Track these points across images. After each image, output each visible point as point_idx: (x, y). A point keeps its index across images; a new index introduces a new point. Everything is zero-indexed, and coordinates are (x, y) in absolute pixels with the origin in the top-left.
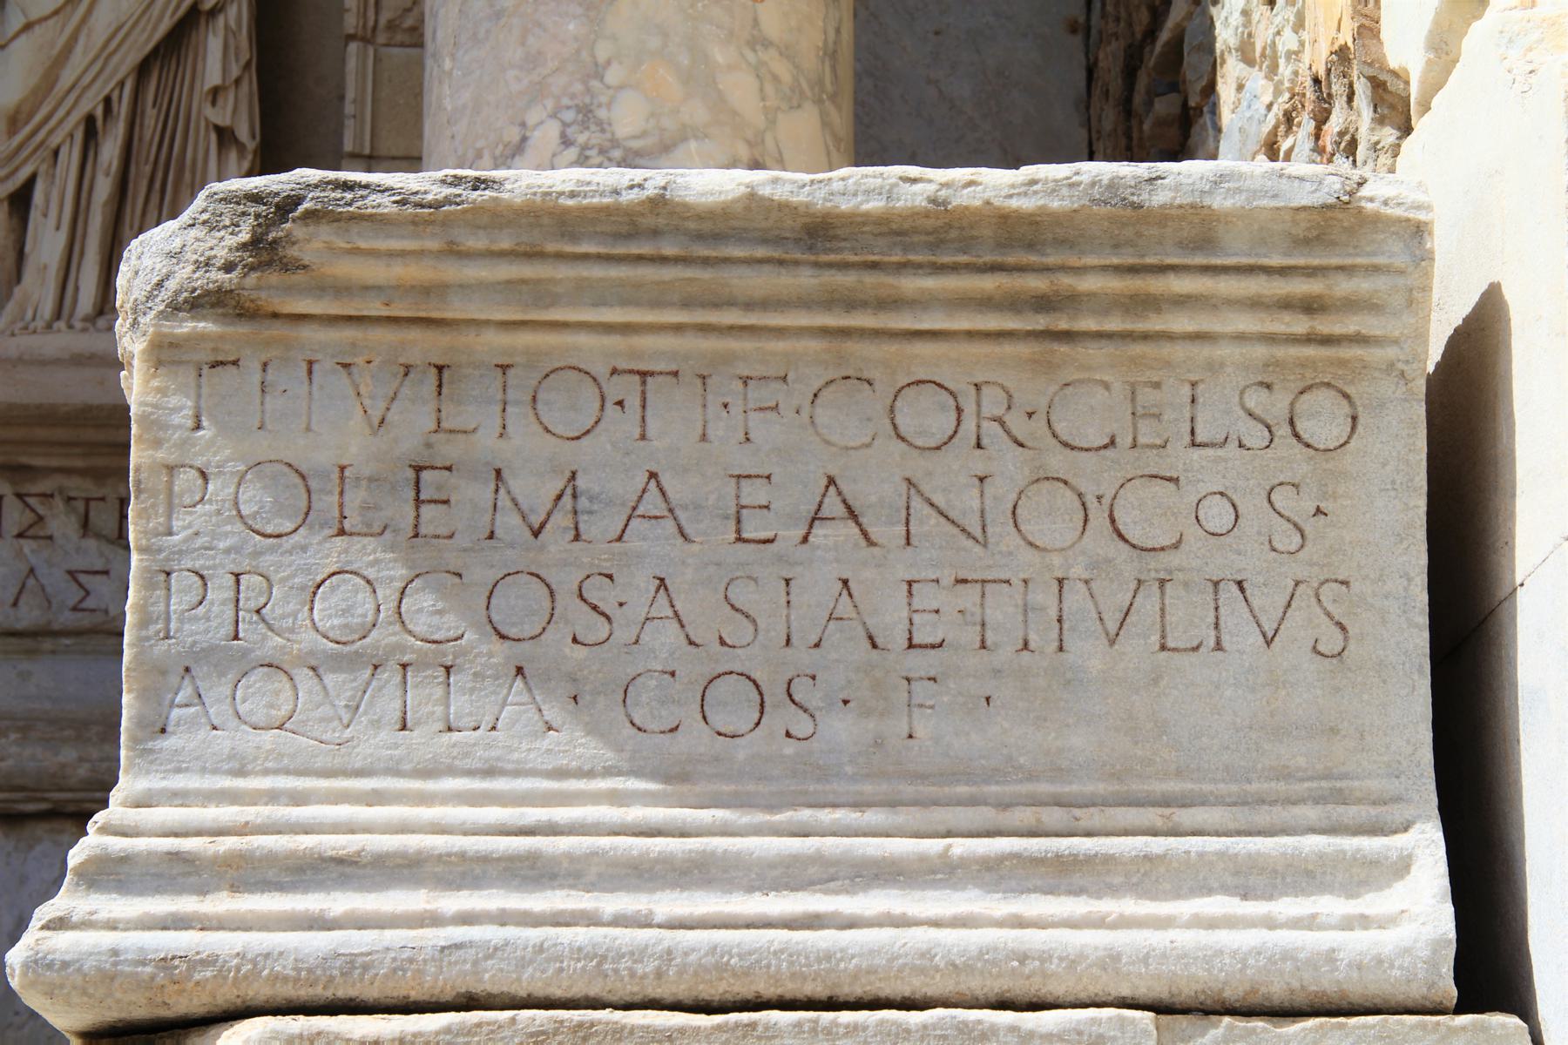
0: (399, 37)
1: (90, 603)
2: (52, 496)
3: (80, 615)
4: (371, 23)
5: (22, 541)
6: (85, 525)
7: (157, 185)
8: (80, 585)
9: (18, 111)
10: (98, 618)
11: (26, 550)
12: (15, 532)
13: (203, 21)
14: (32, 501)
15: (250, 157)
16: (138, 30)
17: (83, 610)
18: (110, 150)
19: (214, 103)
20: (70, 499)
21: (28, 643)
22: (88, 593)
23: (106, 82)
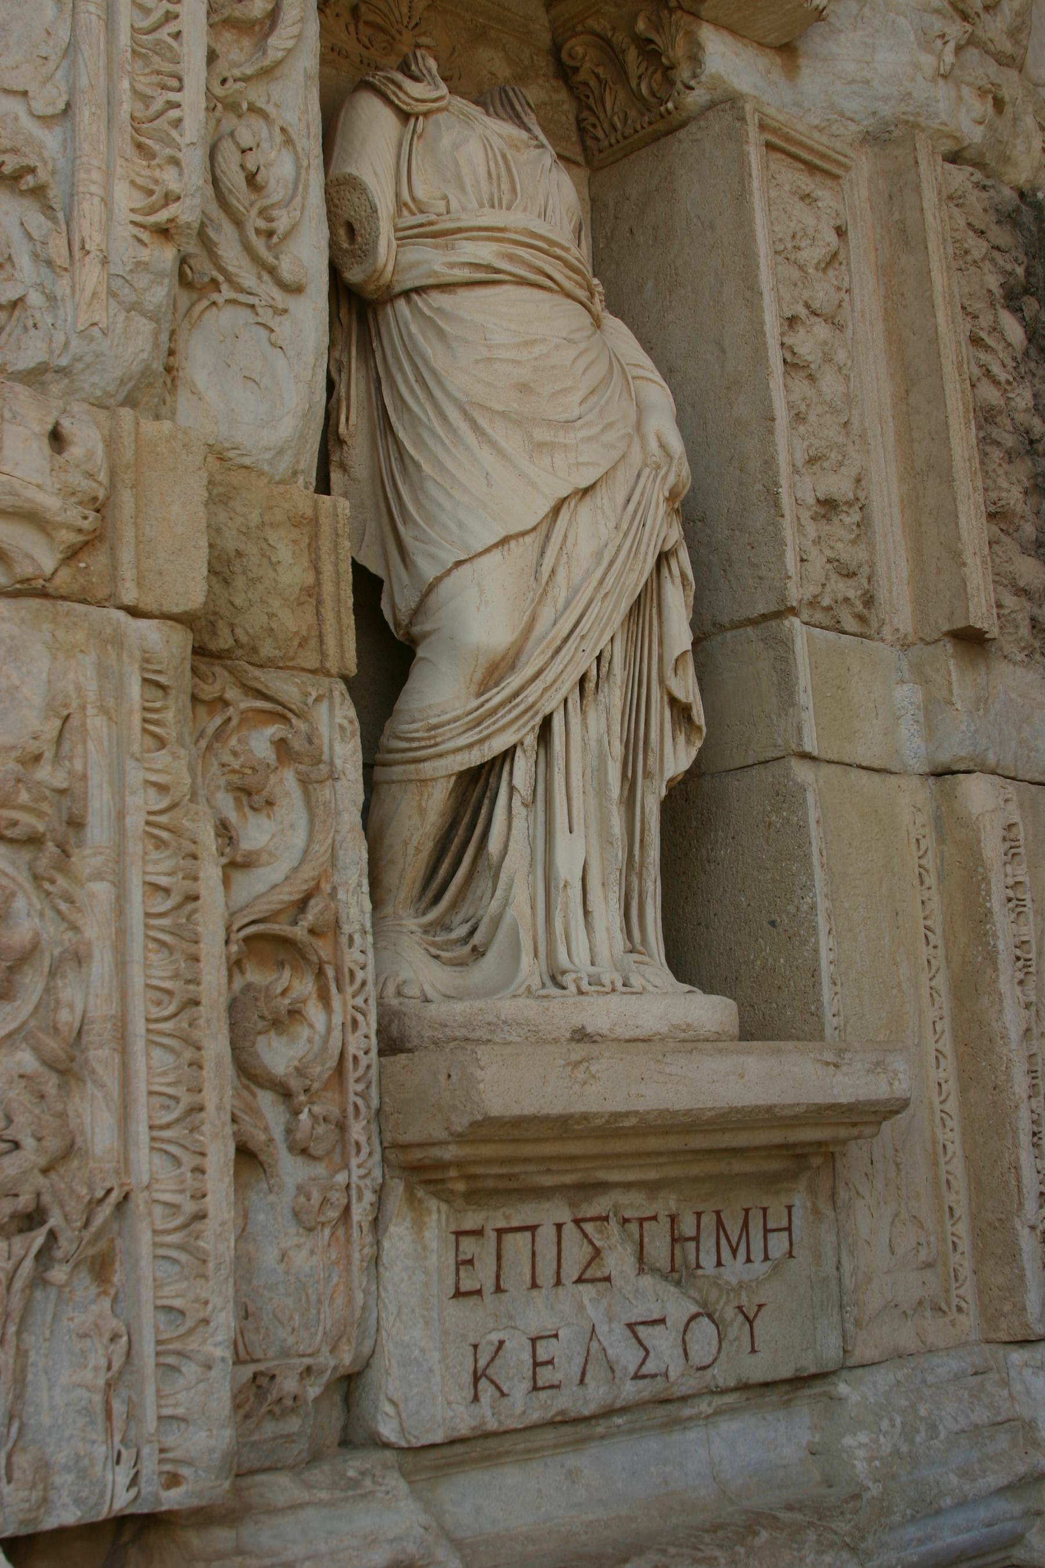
1: (650, 1367)
2: (606, 1219)
3: (641, 1383)
5: (581, 1287)
8: (640, 1342)
10: (659, 1384)
12: (575, 1277)
14: (589, 1227)
15: (699, 744)
17: (644, 1377)
20: (626, 1221)
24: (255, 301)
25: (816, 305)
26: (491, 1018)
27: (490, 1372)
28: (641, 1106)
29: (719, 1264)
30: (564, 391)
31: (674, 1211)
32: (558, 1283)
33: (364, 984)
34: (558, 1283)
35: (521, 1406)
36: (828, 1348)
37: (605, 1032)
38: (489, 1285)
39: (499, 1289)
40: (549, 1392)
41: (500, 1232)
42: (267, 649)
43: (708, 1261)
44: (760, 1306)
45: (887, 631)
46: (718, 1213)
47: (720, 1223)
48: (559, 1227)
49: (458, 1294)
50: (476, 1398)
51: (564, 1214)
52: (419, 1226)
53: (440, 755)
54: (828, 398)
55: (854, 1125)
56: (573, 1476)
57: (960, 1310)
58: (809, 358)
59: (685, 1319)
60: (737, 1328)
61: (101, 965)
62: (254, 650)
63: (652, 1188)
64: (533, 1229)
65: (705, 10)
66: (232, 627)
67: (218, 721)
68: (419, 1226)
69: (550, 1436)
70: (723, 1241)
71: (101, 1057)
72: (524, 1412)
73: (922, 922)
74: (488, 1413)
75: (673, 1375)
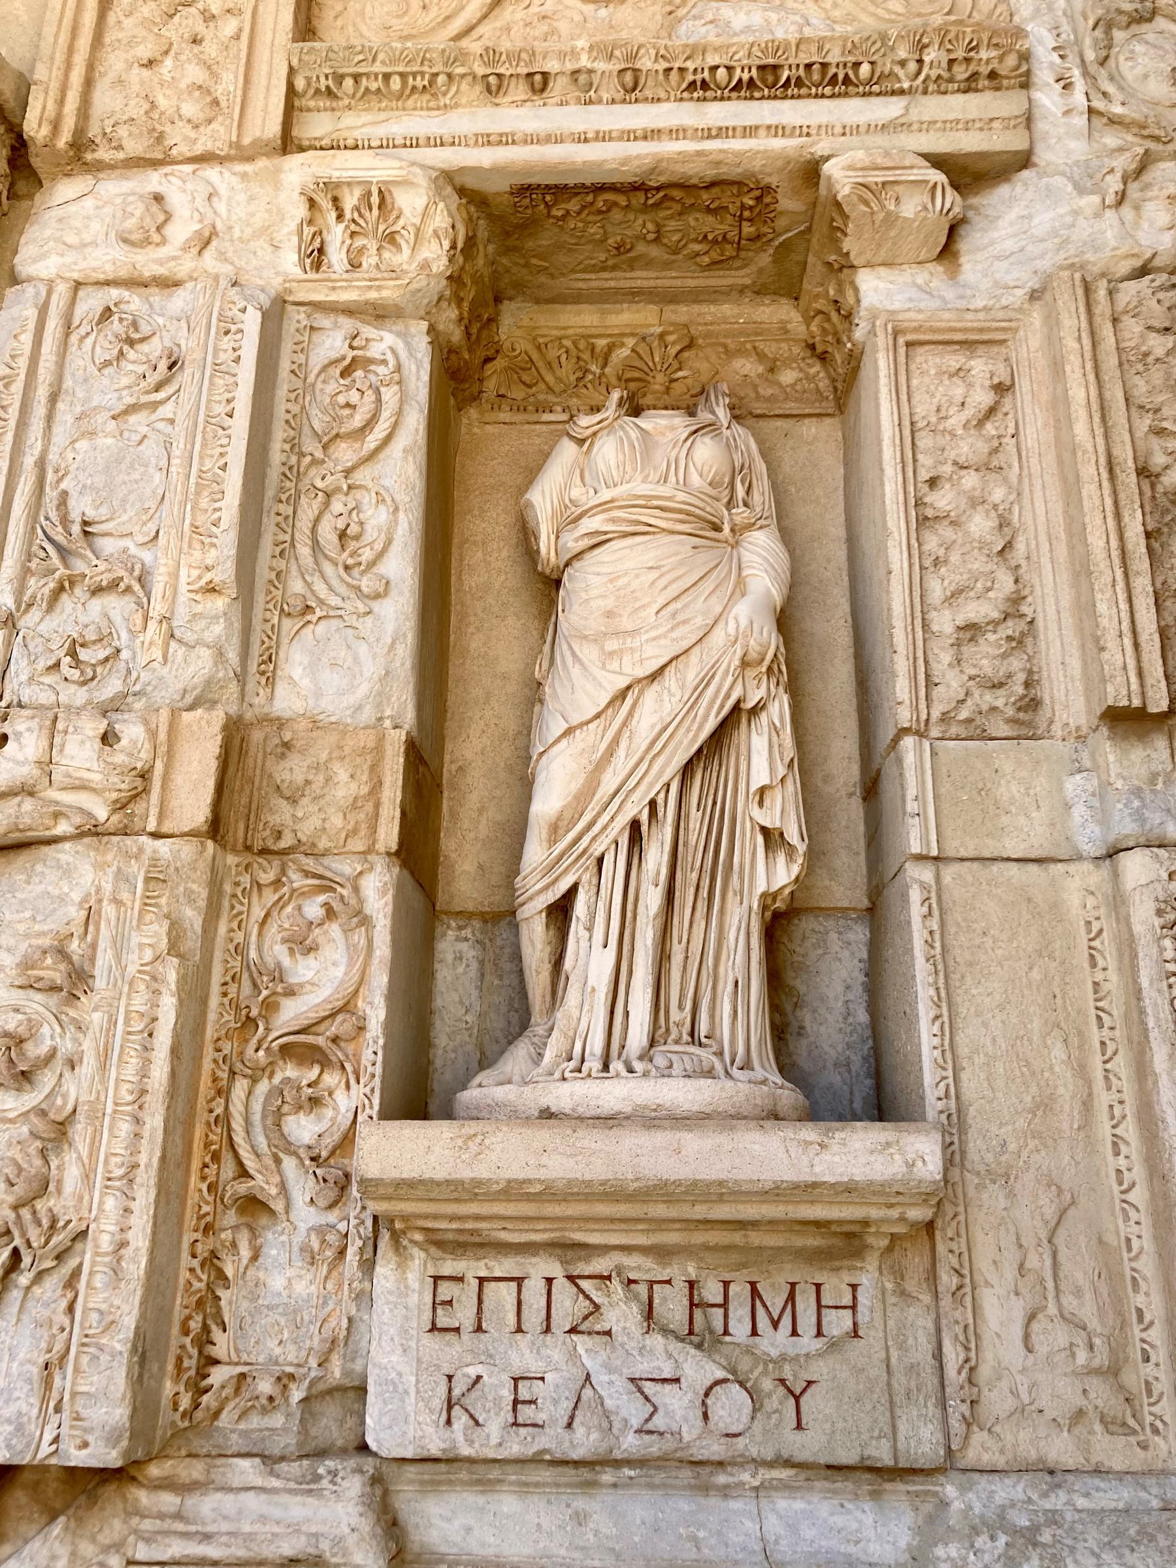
0: (954, 730)
1: (658, 1422)
2: (609, 1278)
3: (647, 1437)
4: (924, 717)
5: (574, 1337)
6: (649, 1314)
7: (704, 893)
8: (647, 1398)
9: (559, 818)
10: (668, 1444)
11: (581, 1350)
13: (744, 720)
14: (584, 1284)
15: (800, 861)
16: (682, 731)
17: (651, 1432)
18: (656, 857)
19: (761, 804)
20: (630, 1282)
21: (585, 1474)
22: (656, 1409)
23: (651, 785)
24: (342, 612)
25: (961, 460)
26: (490, 1101)
27: (466, 1401)
28: (542, 1174)
29: (754, 1333)
30: (643, 607)
31: (693, 1277)
32: (548, 1330)
33: (373, 1076)
34: (548, 1330)
35: (494, 1437)
36: (921, 1439)
37: (567, 1111)
38: (468, 1323)
39: (479, 1329)
40: (530, 1429)
41: (482, 1280)
42: (323, 843)
43: (740, 1329)
44: (810, 1383)
45: (1057, 730)
46: (753, 1285)
47: (755, 1293)
48: (549, 1281)
49: (434, 1328)
50: (449, 1422)
51: (556, 1270)
52: (402, 1266)
53: (531, 898)
54: (977, 536)
55: (891, 1206)
56: (580, 1519)
57: (1156, 1431)
58: (948, 508)
59: (709, 1384)
60: (776, 1399)
61: (88, 1067)
62: (314, 845)
63: (661, 1253)
64: (519, 1281)
65: (855, 259)
66: (295, 831)
67: (276, 897)
68: (402, 1266)
69: (545, 1475)
70: (760, 1311)
71: (80, 1132)
72: (500, 1444)
73: (1092, 1004)
74: (460, 1437)
75: (686, 1437)
